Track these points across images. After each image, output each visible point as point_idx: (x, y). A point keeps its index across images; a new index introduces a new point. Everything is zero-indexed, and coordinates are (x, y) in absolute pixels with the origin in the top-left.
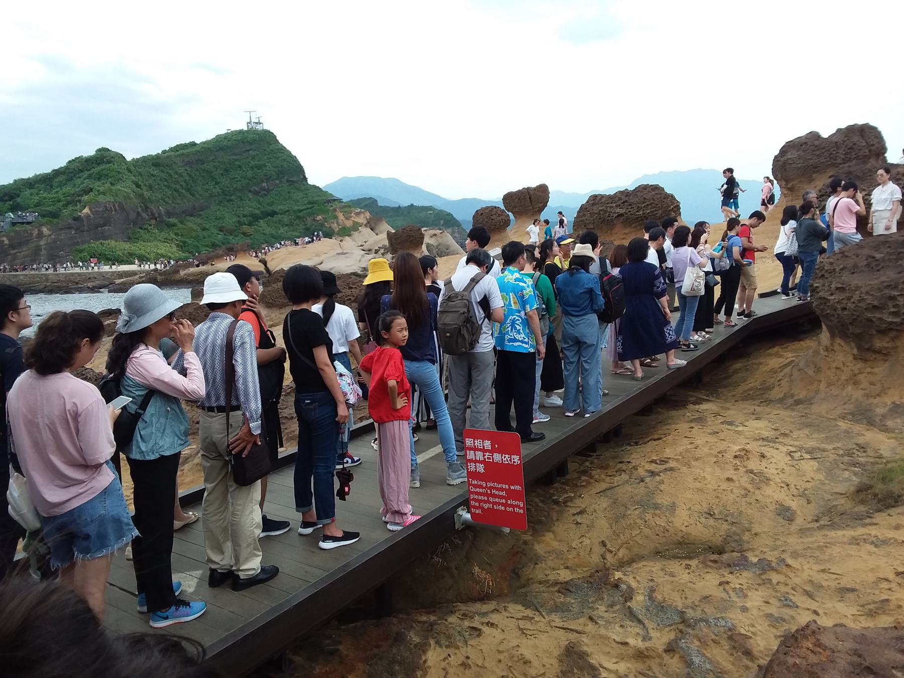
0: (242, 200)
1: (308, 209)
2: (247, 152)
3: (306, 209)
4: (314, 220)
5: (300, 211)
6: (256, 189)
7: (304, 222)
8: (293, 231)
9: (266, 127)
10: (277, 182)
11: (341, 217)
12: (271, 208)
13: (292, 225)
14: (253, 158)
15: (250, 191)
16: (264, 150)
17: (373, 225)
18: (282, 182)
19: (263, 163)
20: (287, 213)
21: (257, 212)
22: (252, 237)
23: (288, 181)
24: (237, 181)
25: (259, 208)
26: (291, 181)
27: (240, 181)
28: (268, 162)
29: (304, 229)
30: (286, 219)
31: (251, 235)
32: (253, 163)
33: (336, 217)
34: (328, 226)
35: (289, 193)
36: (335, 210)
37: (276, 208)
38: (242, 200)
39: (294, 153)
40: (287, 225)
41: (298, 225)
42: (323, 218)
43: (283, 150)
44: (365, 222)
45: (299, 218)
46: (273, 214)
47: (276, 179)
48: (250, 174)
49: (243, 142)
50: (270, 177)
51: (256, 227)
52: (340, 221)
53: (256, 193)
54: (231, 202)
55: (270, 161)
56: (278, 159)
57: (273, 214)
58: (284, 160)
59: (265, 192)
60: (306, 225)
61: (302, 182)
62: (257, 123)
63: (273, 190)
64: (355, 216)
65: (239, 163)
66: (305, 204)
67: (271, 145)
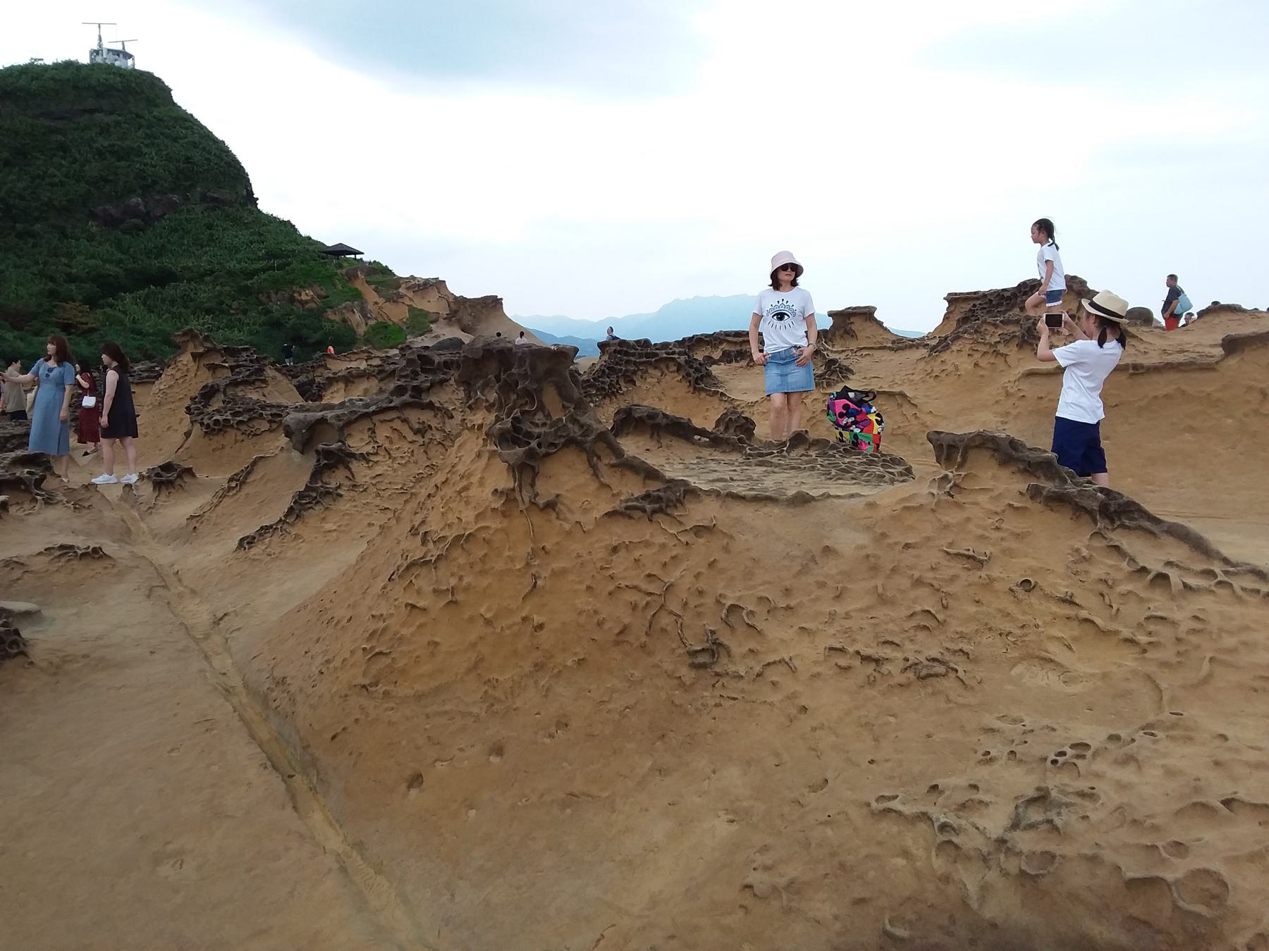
0: (66, 237)
1: (272, 268)
2: (87, 116)
3: (264, 270)
4: (292, 300)
6: (113, 211)
7: (261, 303)
8: (230, 327)
9: (141, 64)
10: (175, 198)
11: (371, 296)
12: (156, 263)
13: (223, 312)
14: (104, 130)
15: (93, 216)
16: (137, 116)
17: (467, 320)
18: (187, 199)
19: (135, 146)
20: (207, 279)
21: (111, 268)
22: (95, 337)
23: (204, 198)
24: (52, 185)
25: (120, 261)
26: (215, 200)
27: (62, 184)
28: (147, 146)
30: (205, 294)
31: (92, 330)
32: (102, 142)
33: (358, 295)
34: (337, 318)
35: (210, 227)
36: (352, 276)
37: (167, 262)
38: (66, 237)
39: (219, 134)
40: (208, 311)
41: (245, 312)
42: (319, 296)
43: (188, 122)
44: (444, 312)
45: (246, 291)
46: (164, 278)
47: (172, 191)
48: (93, 169)
49: (76, 87)
50: (155, 183)
51: (108, 310)
52: (370, 306)
53: (111, 222)
54: (31, 241)
55: (153, 144)
56: (175, 140)
57: (164, 278)
58: (195, 145)
59: (138, 221)
60: (268, 312)
61: (243, 205)
62: (117, 53)
63: (162, 216)
64: (410, 294)
65: (60, 137)
66: (260, 259)
67: (156, 106)
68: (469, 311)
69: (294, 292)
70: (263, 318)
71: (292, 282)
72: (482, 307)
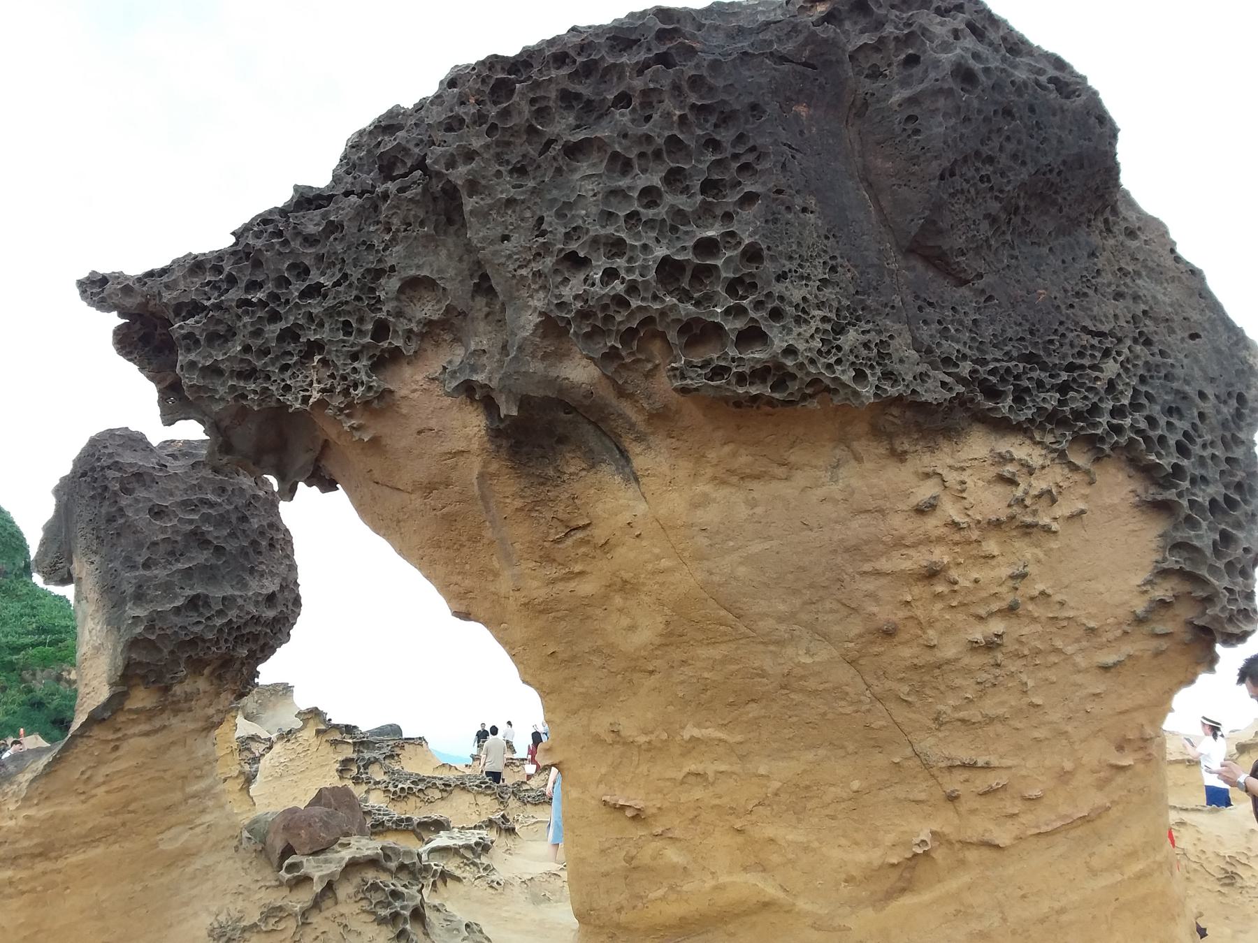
3: (33, 646)
4: (59, 678)
5: (16, 649)
7: (23, 681)
29: (23, 703)
60: (30, 690)
61: (17, 576)
66: (28, 633)
68: (256, 698)
69: (63, 670)
70: (24, 697)
71: (63, 660)
72: (271, 694)
